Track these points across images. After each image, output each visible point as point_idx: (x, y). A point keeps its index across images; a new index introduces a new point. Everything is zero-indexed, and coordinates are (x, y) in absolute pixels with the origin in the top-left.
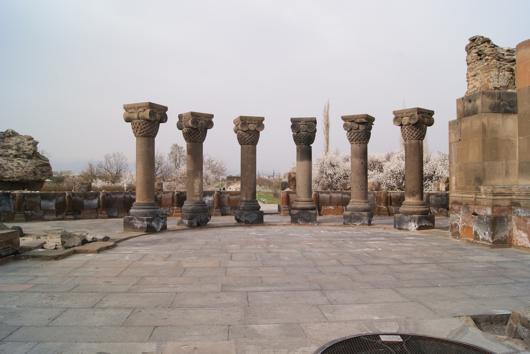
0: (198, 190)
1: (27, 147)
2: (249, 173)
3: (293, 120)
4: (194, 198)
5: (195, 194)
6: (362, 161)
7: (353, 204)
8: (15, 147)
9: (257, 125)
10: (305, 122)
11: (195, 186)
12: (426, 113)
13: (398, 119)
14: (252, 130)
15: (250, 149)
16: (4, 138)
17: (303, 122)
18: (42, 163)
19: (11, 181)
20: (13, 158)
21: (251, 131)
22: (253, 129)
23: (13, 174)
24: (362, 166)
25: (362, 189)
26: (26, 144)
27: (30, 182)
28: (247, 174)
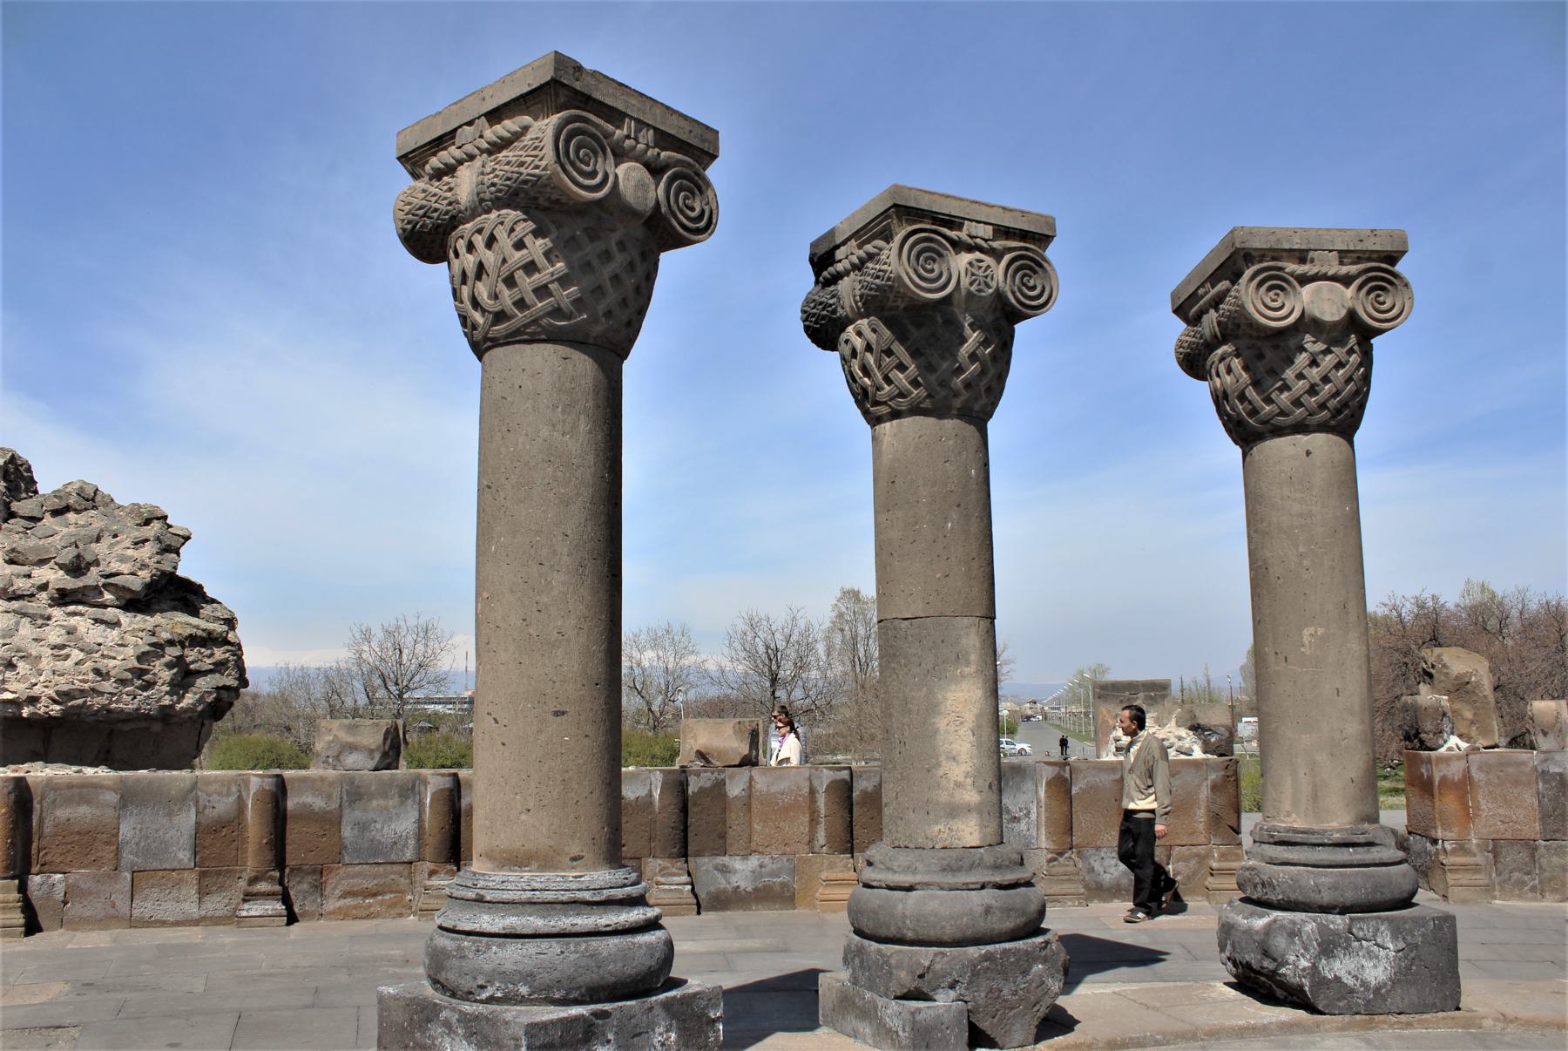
0: (966, 767)
1: (130, 552)
2: (1320, 631)
4: (936, 828)
5: (944, 798)
8: (67, 556)
9: (1360, 288)
15: (1316, 453)
16: (40, 519)
18: (189, 631)
19: (25, 715)
20: (51, 606)
22: (1337, 318)
23: (33, 681)
26: (128, 543)
27: (123, 721)
28: (1306, 640)
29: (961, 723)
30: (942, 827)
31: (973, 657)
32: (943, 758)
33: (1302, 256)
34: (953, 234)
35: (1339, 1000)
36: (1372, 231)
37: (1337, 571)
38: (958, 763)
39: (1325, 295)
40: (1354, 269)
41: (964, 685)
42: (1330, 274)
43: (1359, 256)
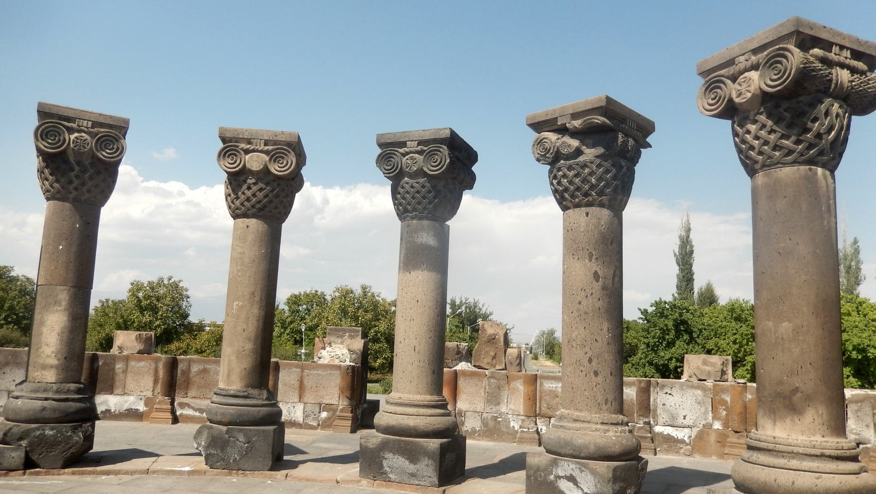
0: (53, 349)
2: (240, 304)
3: (382, 141)
4: (36, 374)
5: (41, 361)
6: (595, 268)
7: (561, 426)
10: (419, 144)
11: (44, 335)
12: (842, 47)
13: (719, 91)
14: (254, 169)
15: (251, 227)
17: (412, 146)
21: (251, 172)
24: (597, 286)
25: (596, 374)
28: (235, 307)
29: (53, 330)
30: (39, 373)
31: (64, 303)
32: (43, 344)
33: (249, 142)
34: (70, 125)
35: (217, 462)
36: (282, 132)
37: (252, 278)
38: (49, 347)
39: (255, 158)
40: (270, 148)
41: (56, 314)
42: (260, 149)
43: (275, 143)
